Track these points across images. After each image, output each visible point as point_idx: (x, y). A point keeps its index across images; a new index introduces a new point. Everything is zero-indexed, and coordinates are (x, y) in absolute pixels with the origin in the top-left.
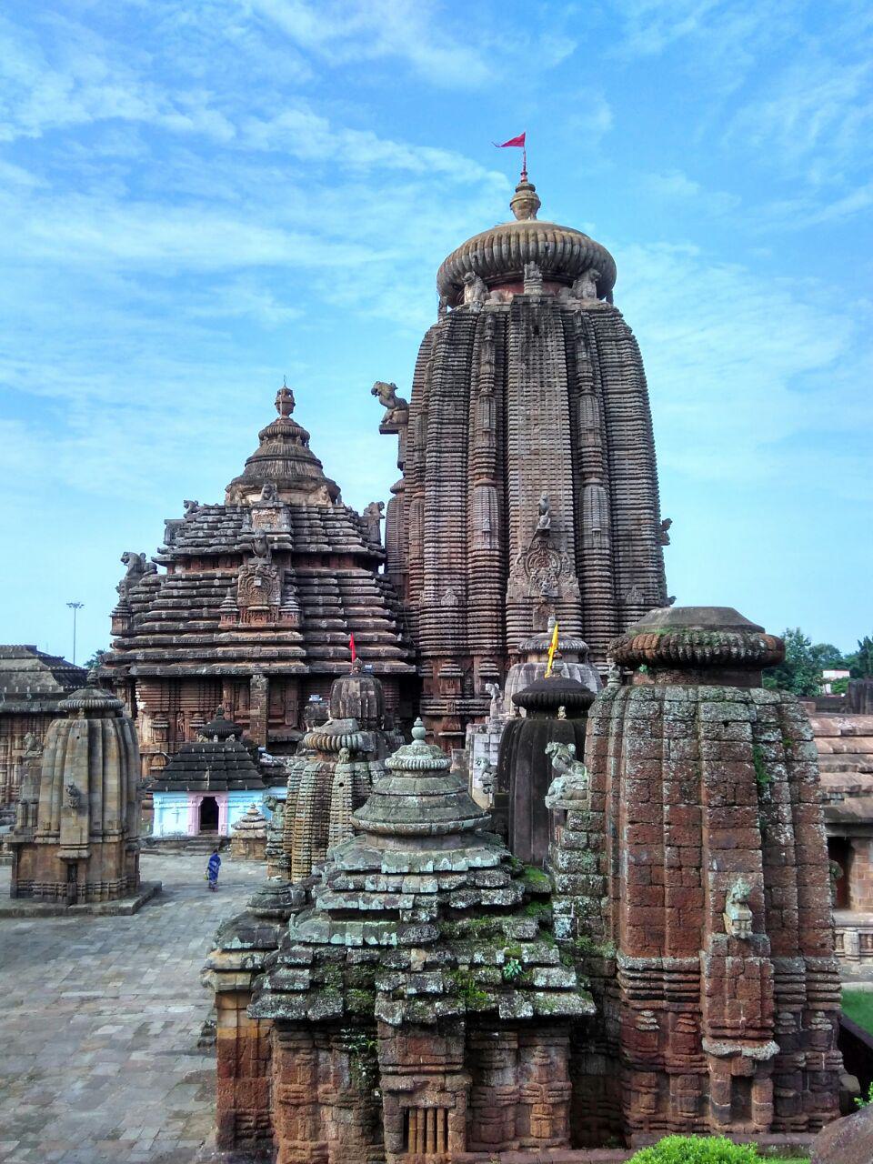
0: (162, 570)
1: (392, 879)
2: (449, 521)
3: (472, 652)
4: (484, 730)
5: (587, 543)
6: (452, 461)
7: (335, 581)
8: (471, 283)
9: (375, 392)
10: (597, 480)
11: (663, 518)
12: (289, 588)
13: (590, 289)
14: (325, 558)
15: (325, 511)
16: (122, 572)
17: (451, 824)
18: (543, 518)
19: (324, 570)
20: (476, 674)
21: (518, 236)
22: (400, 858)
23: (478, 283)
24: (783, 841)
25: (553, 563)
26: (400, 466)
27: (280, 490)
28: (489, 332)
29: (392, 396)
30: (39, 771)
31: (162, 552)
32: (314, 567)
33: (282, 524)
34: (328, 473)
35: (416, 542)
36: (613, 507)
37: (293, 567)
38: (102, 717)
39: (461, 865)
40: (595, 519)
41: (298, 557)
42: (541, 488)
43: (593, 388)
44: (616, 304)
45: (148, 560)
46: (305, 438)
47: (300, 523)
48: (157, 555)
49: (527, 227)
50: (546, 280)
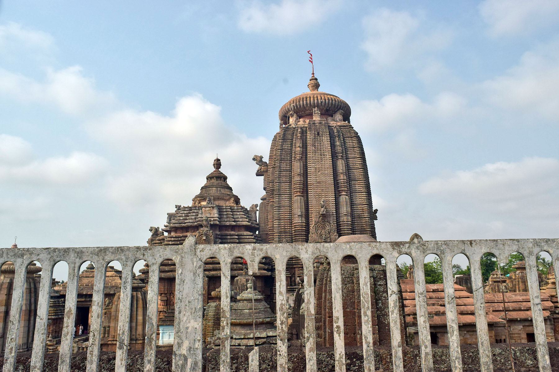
0: (166, 234)
1: (237, 341)
2: (284, 211)
3: (294, 266)
4: (293, 295)
5: (342, 219)
6: (285, 186)
7: (237, 237)
8: (292, 116)
9: (254, 159)
10: (345, 193)
11: (374, 209)
12: (217, 240)
13: (340, 118)
14: (233, 228)
15: (233, 208)
16: (149, 235)
17: (261, 320)
18: (322, 209)
19: (233, 233)
20: (296, 275)
21: (310, 97)
22: (241, 333)
23: (295, 116)
24: (386, 323)
25: (328, 228)
26: (265, 189)
27: (214, 200)
28: (299, 135)
29: (261, 161)
30: (111, 314)
31: (165, 226)
32: (228, 231)
33: (215, 214)
34: (235, 192)
35: (271, 220)
36: (352, 204)
37: (219, 231)
38: (137, 291)
39: (264, 335)
40: (344, 209)
41: (221, 227)
42: (322, 197)
43: (342, 156)
44: (351, 123)
45: (160, 230)
46: (225, 178)
47: (221, 213)
48: (164, 228)
49: (314, 94)
50: (322, 114)
